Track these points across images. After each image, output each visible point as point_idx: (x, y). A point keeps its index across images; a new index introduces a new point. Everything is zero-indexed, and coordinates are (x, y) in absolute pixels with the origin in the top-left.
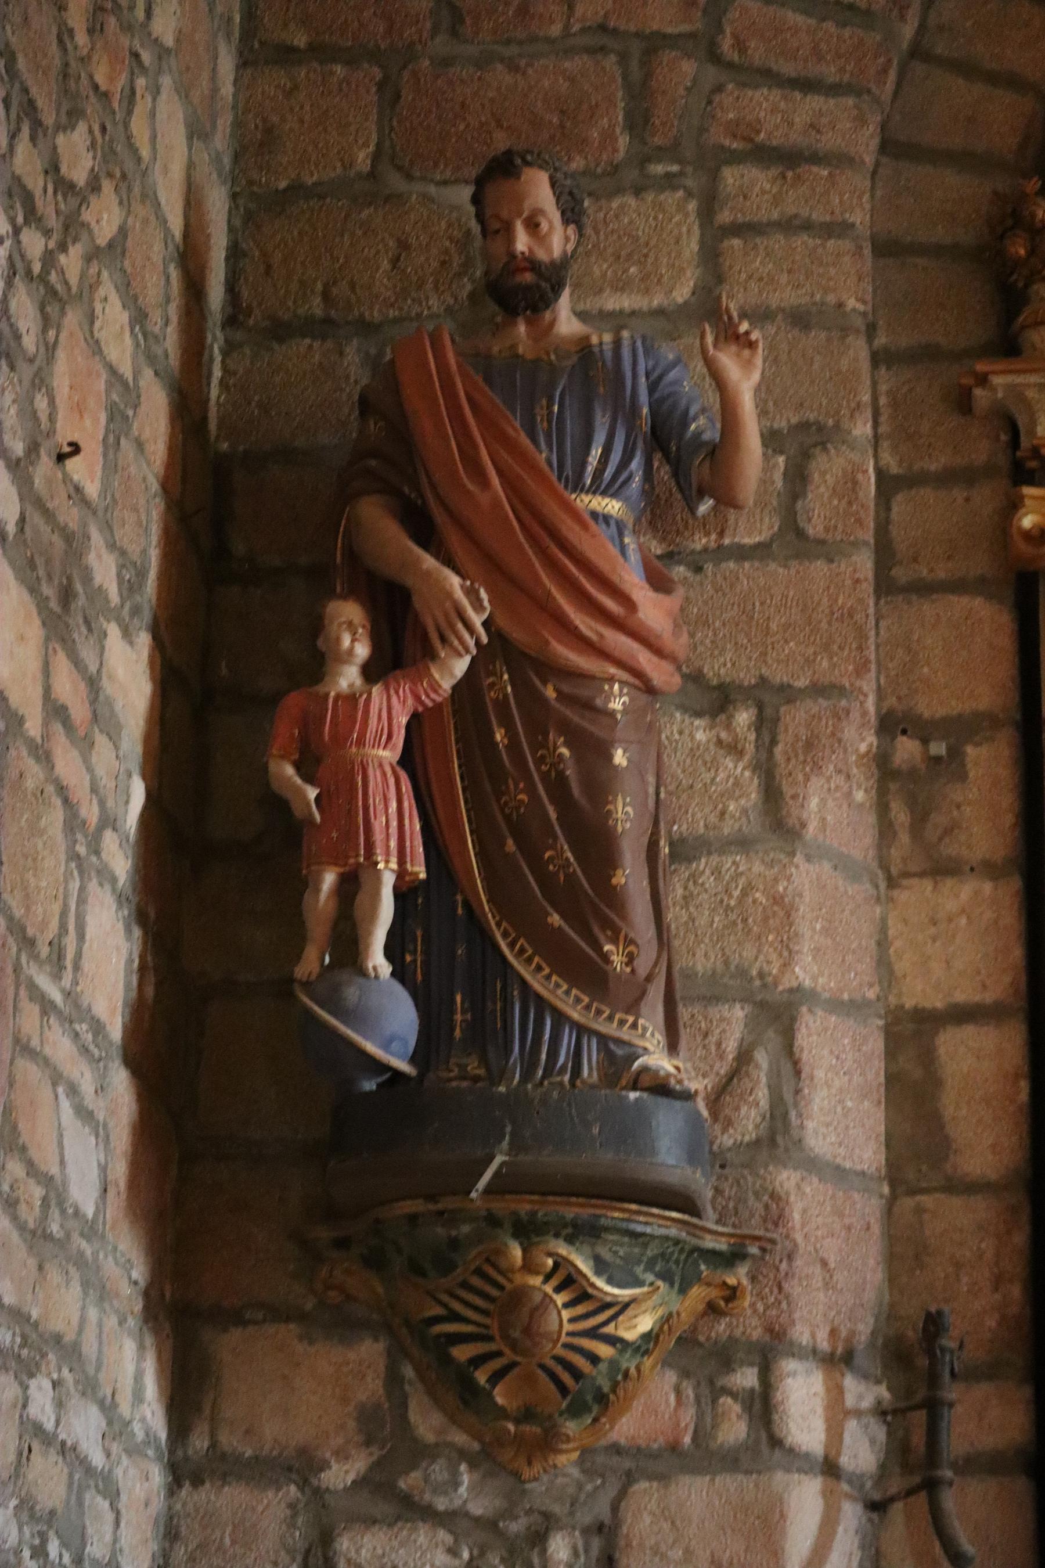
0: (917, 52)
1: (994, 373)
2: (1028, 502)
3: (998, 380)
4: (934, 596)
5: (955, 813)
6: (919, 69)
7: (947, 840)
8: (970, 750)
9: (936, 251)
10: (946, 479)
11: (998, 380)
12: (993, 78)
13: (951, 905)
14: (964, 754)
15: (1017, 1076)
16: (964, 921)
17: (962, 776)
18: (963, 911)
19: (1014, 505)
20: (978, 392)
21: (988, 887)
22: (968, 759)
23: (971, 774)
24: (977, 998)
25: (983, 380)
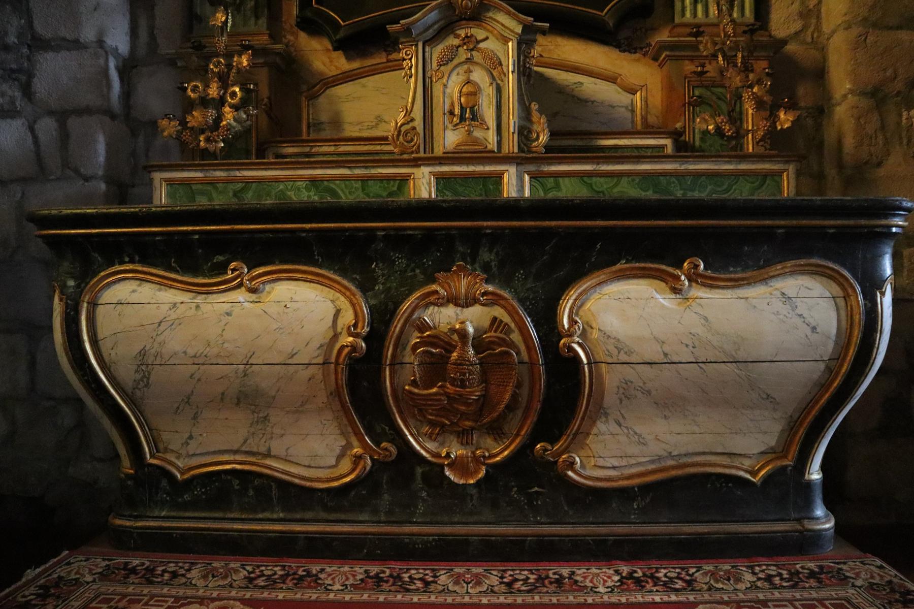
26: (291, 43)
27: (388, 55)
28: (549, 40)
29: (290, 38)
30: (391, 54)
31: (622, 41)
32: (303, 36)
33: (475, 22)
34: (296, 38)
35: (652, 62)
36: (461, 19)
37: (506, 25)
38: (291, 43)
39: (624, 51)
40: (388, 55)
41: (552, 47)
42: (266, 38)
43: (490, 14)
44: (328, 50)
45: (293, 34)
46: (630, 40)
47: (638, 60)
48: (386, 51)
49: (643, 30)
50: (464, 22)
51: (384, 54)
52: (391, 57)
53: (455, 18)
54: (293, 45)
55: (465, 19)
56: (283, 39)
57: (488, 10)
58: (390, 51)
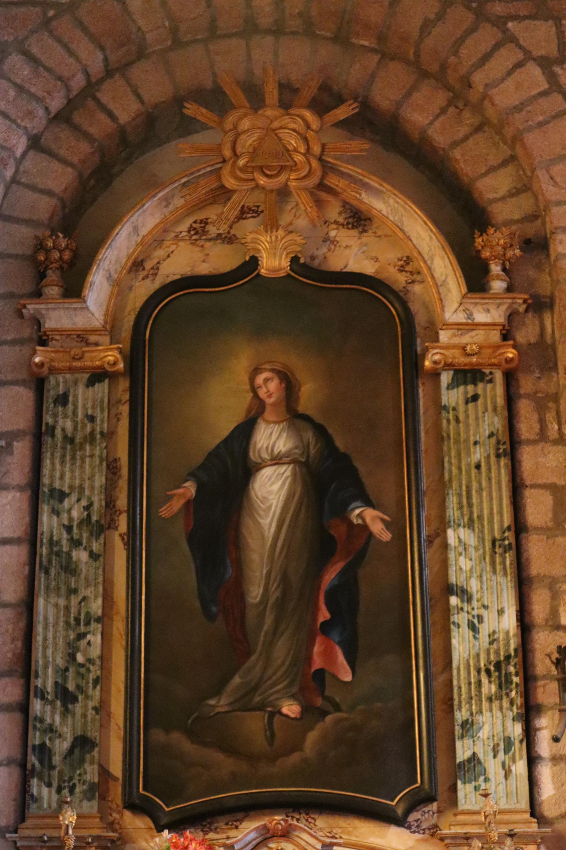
0: (14, 180)
1: (29, 304)
2: (38, 352)
3: (29, 307)
4: (6, 386)
5: (8, 467)
6: (14, 187)
7: (5, 477)
8: (15, 443)
9: (16, 257)
10: (14, 342)
11: (29, 307)
12: (42, 192)
13: (5, 501)
14: (13, 445)
15: (24, 565)
16: (8, 507)
17: (12, 454)
18: (9, 503)
19: (34, 353)
20: (24, 310)
21: (18, 494)
22: (14, 447)
23: (15, 453)
24: (12, 535)
25: (24, 306)
26: (116, 821)
27: (204, 835)
28: (348, 822)
29: (116, 815)
30: (207, 834)
31: (412, 823)
32: (128, 814)
33: (285, 838)
34: (122, 817)
35: (439, 841)
36: (273, 836)
37: (309, 842)
38: (116, 821)
39: (414, 832)
40: (204, 835)
41: (351, 829)
42: (97, 820)
43: (297, 833)
44: (151, 829)
45: (119, 812)
46: (419, 822)
47: (426, 840)
48: (202, 831)
49: (431, 813)
50: (275, 838)
51: (201, 834)
52: (207, 837)
53: (269, 835)
54: (118, 823)
55: (276, 836)
56: (110, 817)
57: (295, 830)
58: (207, 831)
